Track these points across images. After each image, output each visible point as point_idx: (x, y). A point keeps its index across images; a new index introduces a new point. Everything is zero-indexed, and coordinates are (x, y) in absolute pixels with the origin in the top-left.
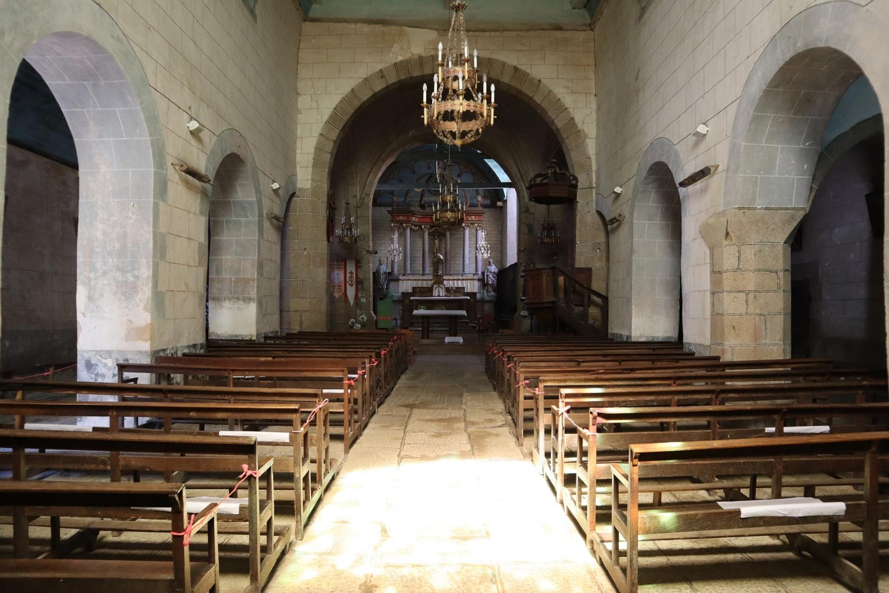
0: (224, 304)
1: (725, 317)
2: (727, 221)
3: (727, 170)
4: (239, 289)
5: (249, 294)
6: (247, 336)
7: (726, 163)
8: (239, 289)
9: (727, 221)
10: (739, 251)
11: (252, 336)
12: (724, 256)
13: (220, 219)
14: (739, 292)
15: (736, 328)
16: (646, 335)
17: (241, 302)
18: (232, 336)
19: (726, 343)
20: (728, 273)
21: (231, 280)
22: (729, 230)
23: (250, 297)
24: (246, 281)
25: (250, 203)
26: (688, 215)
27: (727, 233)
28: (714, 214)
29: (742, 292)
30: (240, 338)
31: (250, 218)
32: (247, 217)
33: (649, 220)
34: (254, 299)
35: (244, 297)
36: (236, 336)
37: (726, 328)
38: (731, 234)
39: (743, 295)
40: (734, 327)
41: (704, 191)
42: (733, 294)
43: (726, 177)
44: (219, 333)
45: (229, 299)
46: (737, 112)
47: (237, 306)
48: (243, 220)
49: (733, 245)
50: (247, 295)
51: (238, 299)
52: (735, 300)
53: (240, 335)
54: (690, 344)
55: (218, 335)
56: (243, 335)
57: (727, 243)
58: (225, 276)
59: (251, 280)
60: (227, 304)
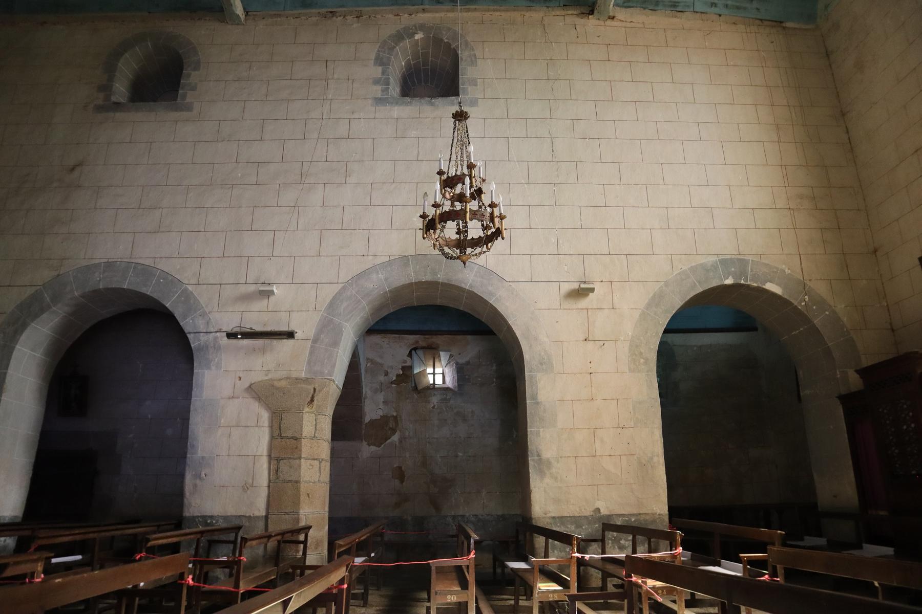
1: (301, 485)
2: (315, 389)
3: (315, 341)
7: (311, 334)
9: (315, 389)
12: (304, 422)
14: (314, 459)
15: (310, 496)
19: (301, 511)
20: (306, 440)
22: (315, 399)
26: (213, 368)
27: (312, 400)
28: (287, 378)
29: (316, 459)
33: (32, 350)
37: (301, 496)
38: (315, 402)
39: (317, 463)
40: (308, 495)
41: (263, 351)
42: (309, 461)
43: (312, 347)
46: (340, 293)
52: (311, 467)
54: (212, 517)
57: (306, 409)
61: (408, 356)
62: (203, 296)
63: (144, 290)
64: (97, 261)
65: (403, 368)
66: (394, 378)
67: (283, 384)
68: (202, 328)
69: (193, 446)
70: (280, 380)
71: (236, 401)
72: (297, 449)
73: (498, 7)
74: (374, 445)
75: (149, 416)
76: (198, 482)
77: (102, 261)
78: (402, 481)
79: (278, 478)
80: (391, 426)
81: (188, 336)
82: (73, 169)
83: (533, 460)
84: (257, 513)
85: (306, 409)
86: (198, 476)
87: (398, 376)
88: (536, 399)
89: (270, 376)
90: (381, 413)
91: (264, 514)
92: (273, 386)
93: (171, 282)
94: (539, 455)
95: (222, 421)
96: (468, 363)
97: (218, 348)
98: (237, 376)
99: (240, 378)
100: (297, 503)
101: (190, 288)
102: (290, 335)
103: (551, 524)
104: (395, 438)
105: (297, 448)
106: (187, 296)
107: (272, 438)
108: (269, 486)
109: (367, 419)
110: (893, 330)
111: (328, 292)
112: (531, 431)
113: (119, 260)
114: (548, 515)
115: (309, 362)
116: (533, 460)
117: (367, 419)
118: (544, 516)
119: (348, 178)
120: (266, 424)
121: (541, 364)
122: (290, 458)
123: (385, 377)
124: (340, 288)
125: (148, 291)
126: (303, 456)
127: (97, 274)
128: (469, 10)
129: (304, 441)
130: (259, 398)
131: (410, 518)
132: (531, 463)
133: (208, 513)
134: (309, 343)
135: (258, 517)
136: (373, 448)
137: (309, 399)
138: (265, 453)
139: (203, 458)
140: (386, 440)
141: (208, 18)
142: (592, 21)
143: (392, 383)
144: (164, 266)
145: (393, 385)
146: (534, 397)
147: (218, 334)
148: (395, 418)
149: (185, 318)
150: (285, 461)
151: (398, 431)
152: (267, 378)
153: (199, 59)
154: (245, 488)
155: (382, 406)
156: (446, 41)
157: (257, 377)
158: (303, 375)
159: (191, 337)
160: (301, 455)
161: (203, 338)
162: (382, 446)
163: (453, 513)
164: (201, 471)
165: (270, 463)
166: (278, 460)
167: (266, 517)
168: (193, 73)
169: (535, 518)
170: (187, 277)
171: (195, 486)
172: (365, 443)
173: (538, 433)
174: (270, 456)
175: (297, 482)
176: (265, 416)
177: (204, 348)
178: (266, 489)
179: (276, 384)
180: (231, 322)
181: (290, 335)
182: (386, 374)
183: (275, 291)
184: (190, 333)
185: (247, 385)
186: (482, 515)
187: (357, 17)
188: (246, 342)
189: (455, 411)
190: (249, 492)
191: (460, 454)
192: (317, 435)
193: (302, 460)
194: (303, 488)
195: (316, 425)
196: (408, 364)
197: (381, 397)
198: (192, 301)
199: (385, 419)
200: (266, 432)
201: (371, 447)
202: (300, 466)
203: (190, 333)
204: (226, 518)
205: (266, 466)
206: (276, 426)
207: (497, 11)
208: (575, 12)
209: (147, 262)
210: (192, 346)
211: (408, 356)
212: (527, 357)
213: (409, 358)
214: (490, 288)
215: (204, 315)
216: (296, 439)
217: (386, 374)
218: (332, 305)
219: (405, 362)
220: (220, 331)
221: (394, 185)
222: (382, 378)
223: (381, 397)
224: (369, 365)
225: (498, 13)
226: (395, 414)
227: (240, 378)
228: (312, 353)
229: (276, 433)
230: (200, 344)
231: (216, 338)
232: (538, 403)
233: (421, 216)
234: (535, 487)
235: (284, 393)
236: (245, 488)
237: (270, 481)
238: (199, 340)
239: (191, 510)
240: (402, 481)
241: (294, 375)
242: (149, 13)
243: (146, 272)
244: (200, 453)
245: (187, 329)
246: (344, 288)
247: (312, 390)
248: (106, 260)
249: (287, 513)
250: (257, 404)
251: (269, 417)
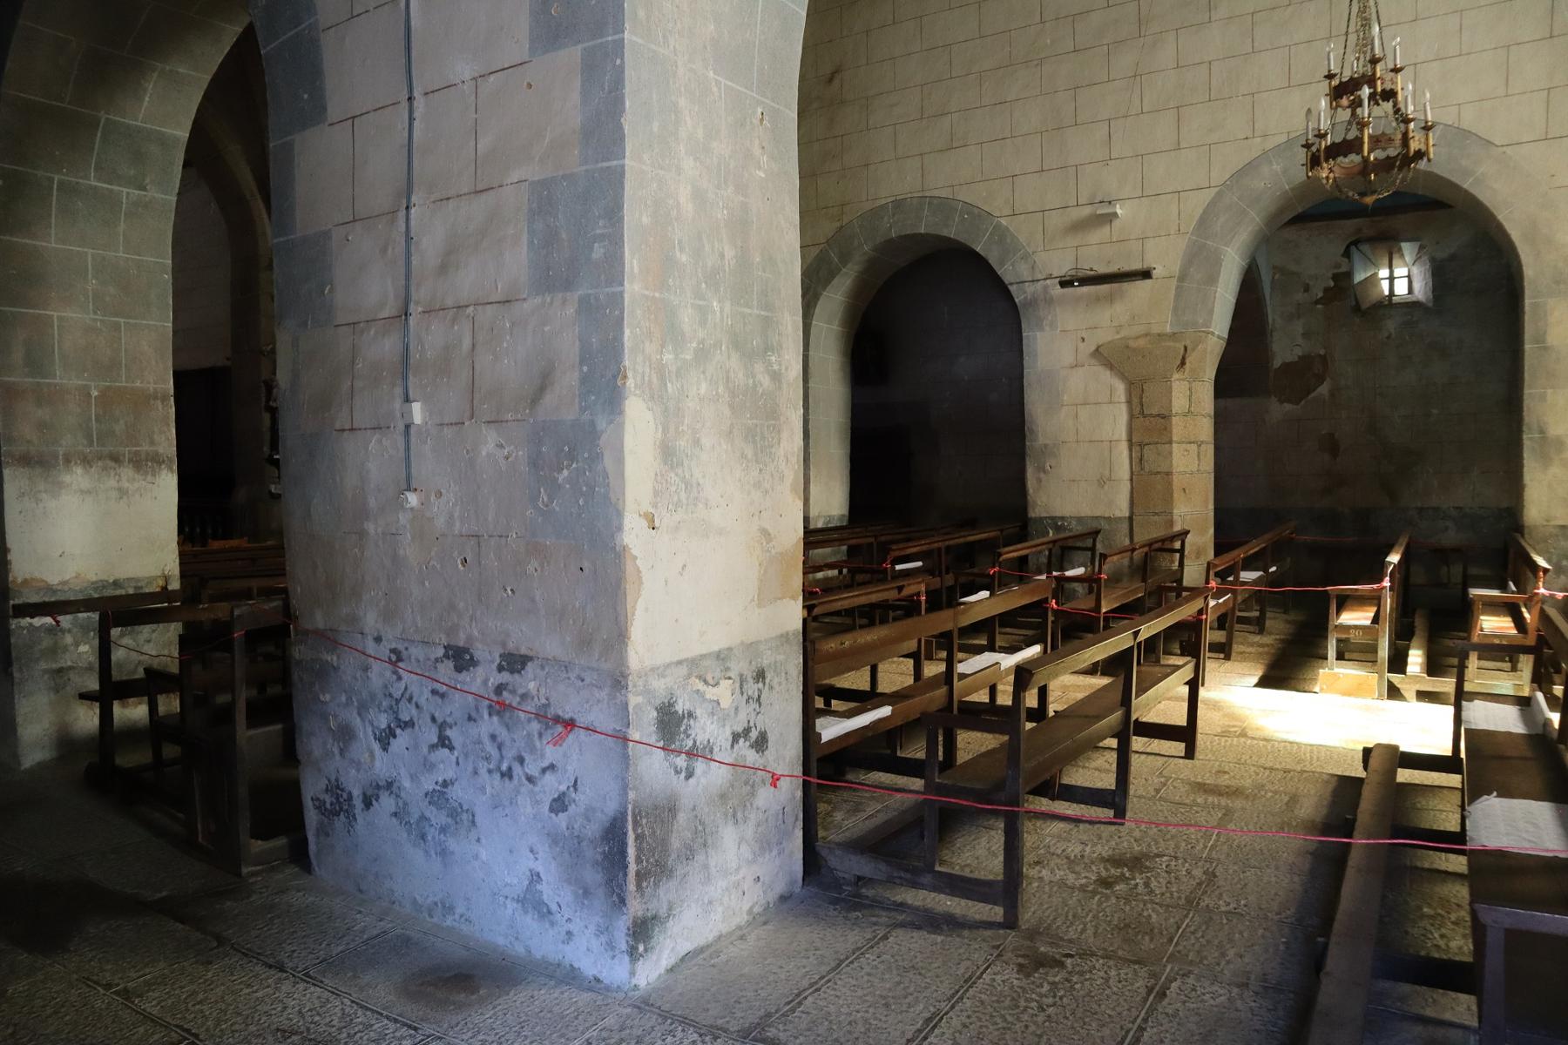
0: (67, 478)
3: (1182, 278)
4: (119, 428)
5: (152, 443)
6: (151, 580)
7: (1176, 269)
8: (119, 428)
10: (1190, 389)
11: (167, 579)
12: (1173, 394)
13: (40, 173)
14: (1190, 443)
16: (824, 514)
17: (127, 472)
18: (104, 585)
19: (1175, 511)
21: (89, 395)
22: (1187, 361)
23: (157, 454)
24: (141, 401)
25: (164, 142)
26: (1047, 328)
27: (1183, 363)
28: (1146, 335)
30: (131, 591)
31: (154, 193)
32: (144, 189)
34: (170, 460)
35: (136, 453)
36: (116, 584)
38: (1188, 364)
39: (1194, 447)
41: (1111, 299)
43: (1177, 288)
44: (54, 580)
45: (86, 461)
46: (1213, 203)
47: (112, 483)
48: (126, 193)
49: (1183, 380)
50: (145, 448)
51: (116, 459)
53: (129, 579)
54: (1062, 518)
55: (50, 589)
56: (137, 580)
57: (1176, 376)
58: (63, 378)
59: (156, 398)
60: (77, 477)
61: (1343, 255)
62: (1022, 231)
63: (945, 233)
64: (883, 202)
65: (1335, 277)
66: (1320, 295)
67: (1141, 342)
68: (1026, 276)
69: (1032, 431)
70: (1137, 338)
71: (1080, 370)
72: (1166, 430)
74: (1289, 401)
75: (966, 378)
76: (1042, 475)
77: (890, 200)
80: (1316, 372)
81: (1010, 288)
82: (831, 80)
83: (1531, 439)
84: (1118, 514)
85: (1176, 376)
87: (1326, 290)
88: (1544, 342)
89: (1122, 334)
90: (1298, 352)
91: (1127, 515)
92: (1127, 347)
93: (977, 216)
94: (1542, 431)
95: (1065, 398)
96: (1453, 257)
97: (1050, 301)
98: (1079, 337)
99: (1083, 339)
100: (1168, 498)
101: (1004, 222)
102: (1146, 274)
103: (1557, 536)
104: (1324, 389)
105: (1165, 429)
106: (1001, 235)
107: (1132, 417)
108: (1131, 480)
109: (1277, 363)
111: (1197, 204)
112: (1530, 394)
113: (909, 195)
114: (1553, 523)
115: (1175, 309)
116: (1531, 439)
117: (1277, 363)
118: (1545, 523)
119: (1213, 12)
120: (1123, 398)
121: (1557, 283)
122: (1157, 443)
123: (1306, 294)
124: (1213, 195)
125: (951, 232)
126: (1175, 439)
127: (886, 219)
129: (1175, 420)
130: (1110, 366)
132: (1527, 444)
133: (1058, 514)
134: (1174, 283)
135: (1120, 518)
136: (1288, 407)
137: (1179, 362)
138: (1124, 436)
140: (1309, 393)
143: (1317, 302)
144: (964, 195)
145: (1319, 306)
146: (1540, 339)
147: (1048, 281)
148: (1323, 359)
149: (1002, 263)
150: (1151, 447)
151: (1328, 379)
152: (1118, 336)
154: (1102, 482)
155: (1300, 341)
157: (1104, 336)
158: (1168, 329)
160: (1171, 437)
161: (1030, 289)
162: (1303, 402)
163: (1419, 505)
164: (1045, 463)
165: (1131, 450)
166: (1142, 445)
167: (1131, 519)
169: (1528, 527)
170: (997, 206)
171: (1039, 480)
172: (1274, 399)
173: (1543, 398)
174: (1130, 440)
175: (1169, 474)
176: (1120, 388)
177: (1032, 303)
179: (1132, 344)
180: (1063, 264)
181: (1146, 274)
182: (1307, 289)
183: (1119, 211)
184: (1011, 284)
185: (1093, 348)
186: (1471, 508)
188: (1085, 289)
190: (1106, 487)
191: (1435, 411)
192: (1192, 409)
193: (1174, 445)
194: (1177, 481)
195: (1190, 396)
196: (1343, 269)
197: (1298, 327)
198: (1008, 241)
199: (1306, 360)
200: (1124, 408)
201: (1285, 404)
202: (1171, 453)
203: (1011, 284)
204: (1080, 519)
205: (1126, 453)
206: (1135, 401)
210: (1017, 300)
211: (1343, 255)
212: (1529, 272)
213: (1347, 260)
214: (1464, 162)
215: (1026, 257)
216: (1163, 417)
217: (1307, 289)
218: (1203, 222)
219: (1338, 266)
220: (1050, 277)
221: (1290, 8)
222: (1300, 296)
223: (1298, 327)
224: (1277, 277)
226: (1322, 352)
227: (1083, 339)
228: (1177, 296)
229: (1137, 410)
230: (1025, 298)
231: (1046, 288)
232: (1546, 348)
233: (1303, 146)
234: (1531, 480)
235: (1143, 357)
236: (1102, 482)
238: (1025, 292)
239: (1036, 510)
241: (1156, 330)
243: (944, 206)
244: (1041, 440)
245: (1007, 279)
246: (1219, 195)
247: (1183, 349)
248: (894, 199)
249: (1156, 514)
250: (1108, 372)
251: (1126, 389)
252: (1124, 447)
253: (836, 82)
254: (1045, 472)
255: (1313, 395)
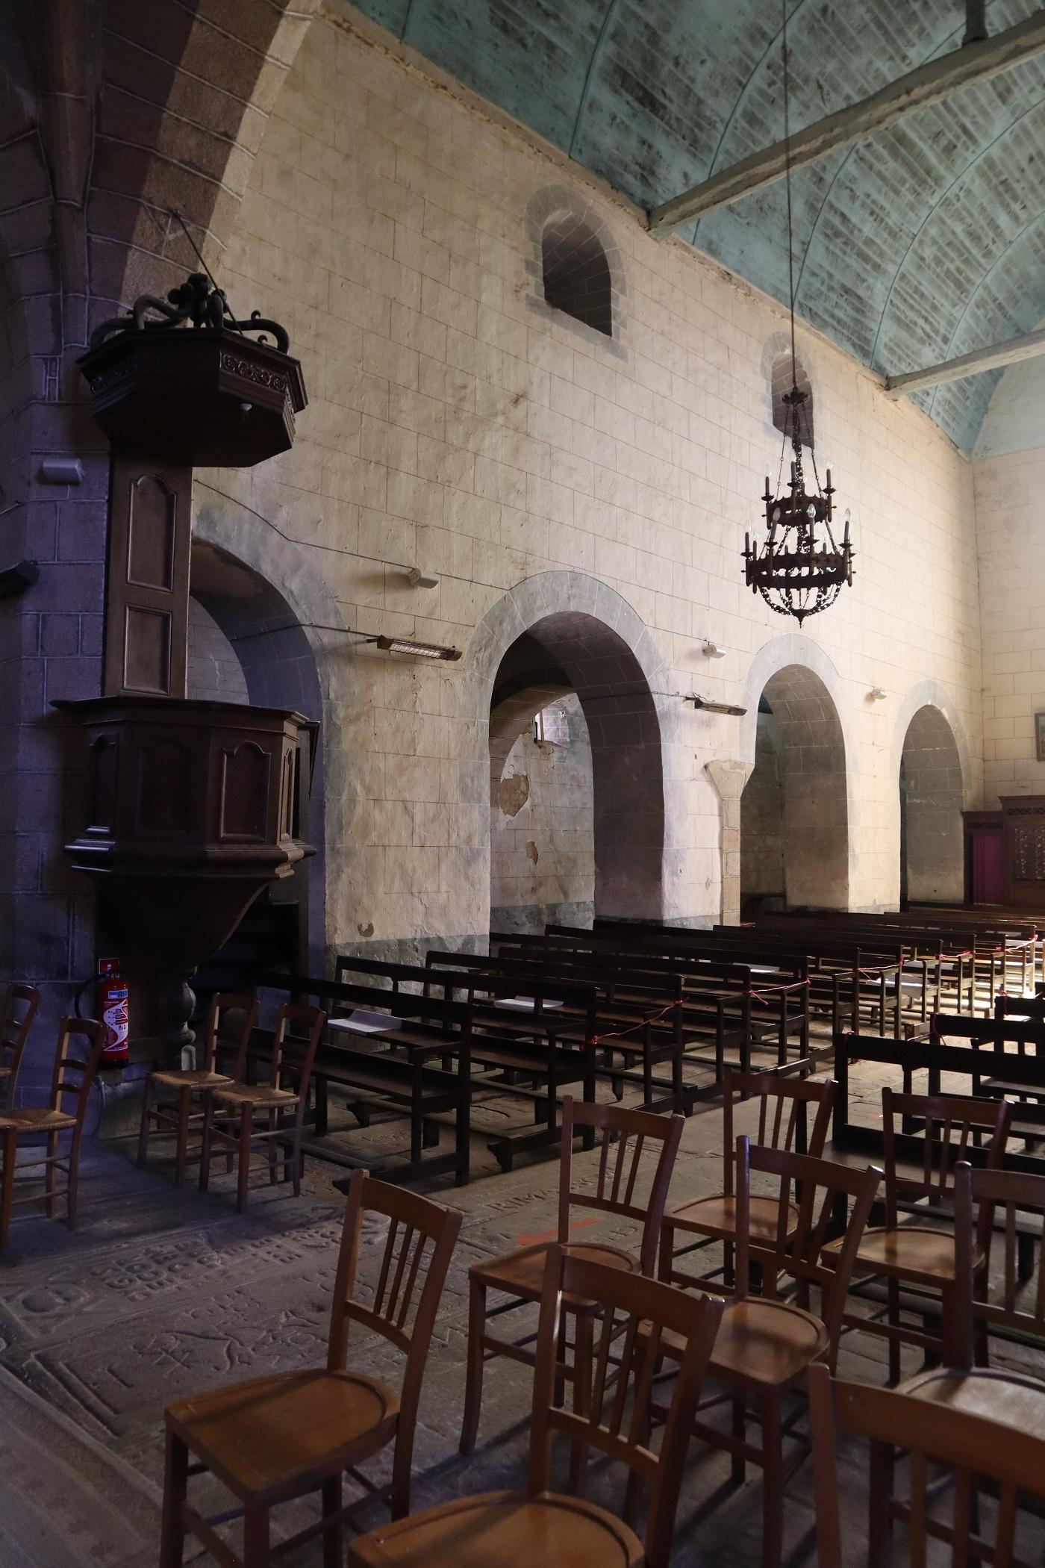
26: (676, 741)
41: (708, 724)
68: (663, 689)
73: (836, 345)
76: (675, 879)
78: (536, 862)
79: (727, 873)
86: (674, 873)
91: (717, 912)
97: (678, 717)
99: (696, 757)
101: (650, 631)
104: (527, 805)
107: (722, 829)
108: (722, 882)
110: (984, 760)
125: (614, 625)
128: (819, 338)
130: (712, 781)
131: (544, 907)
139: (678, 851)
141: (628, 210)
142: (881, 396)
153: (624, 276)
156: (804, 369)
159: (655, 697)
165: (721, 856)
168: (622, 297)
171: (674, 884)
172: (501, 810)
174: (721, 848)
176: (715, 801)
178: (719, 885)
185: (702, 766)
187: (746, 294)
189: (571, 773)
207: (834, 348)
208: (876, 381)
209: (610, 583)
210: (657, 710)
225: (835, 353)
231: (676, 703)
236: (708, 884)
237: (722, 877)
240: (536, 862)
242: (570, 157)
244: (675, 846)
245: (653, 688)
252: (717, 851)
253: (523, 405)
254: (677, 876)
255: (522, 809)
